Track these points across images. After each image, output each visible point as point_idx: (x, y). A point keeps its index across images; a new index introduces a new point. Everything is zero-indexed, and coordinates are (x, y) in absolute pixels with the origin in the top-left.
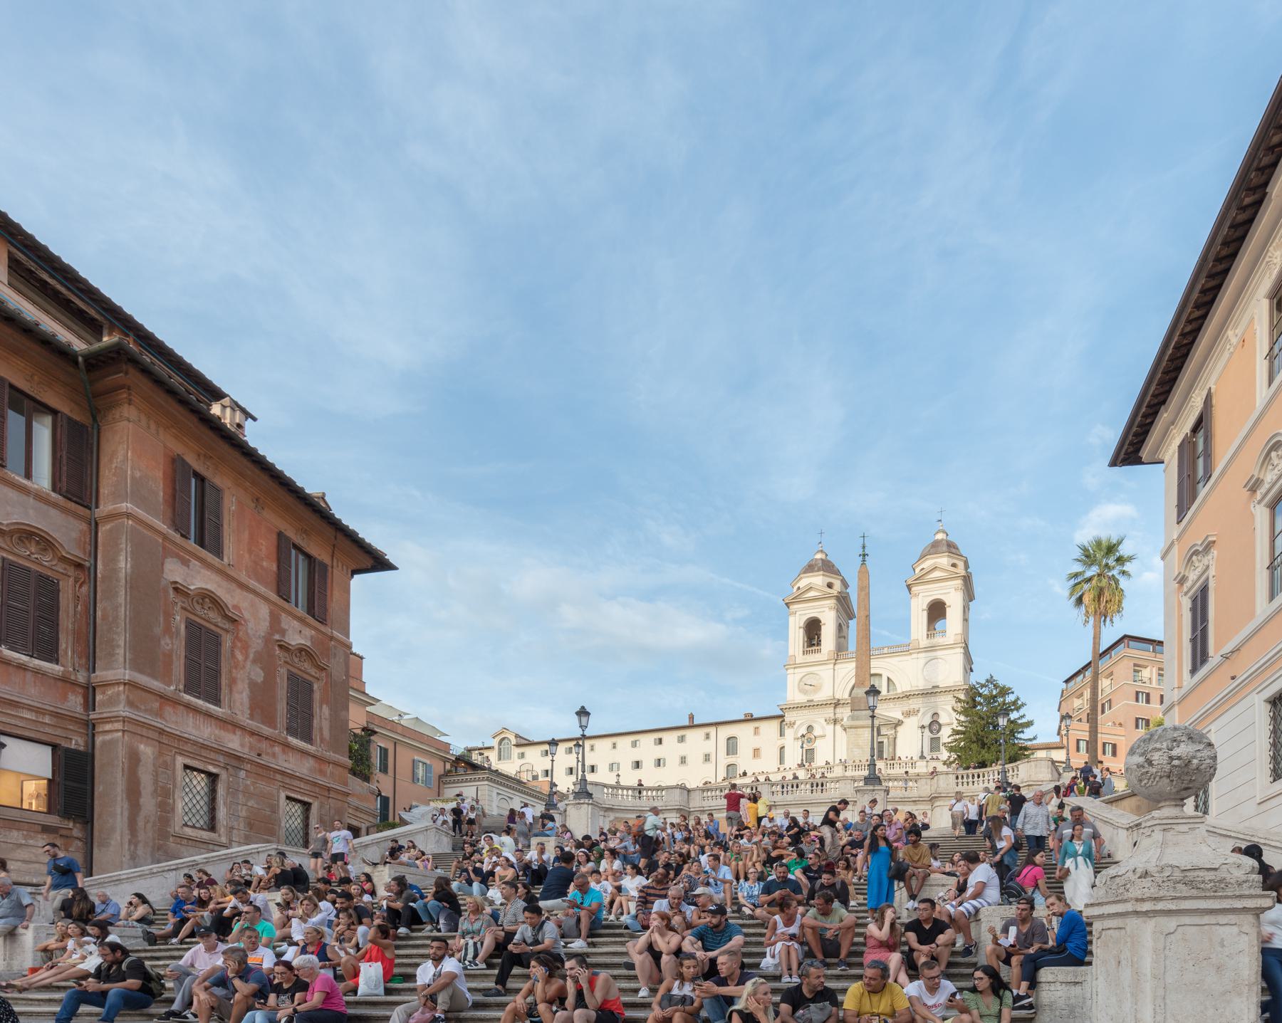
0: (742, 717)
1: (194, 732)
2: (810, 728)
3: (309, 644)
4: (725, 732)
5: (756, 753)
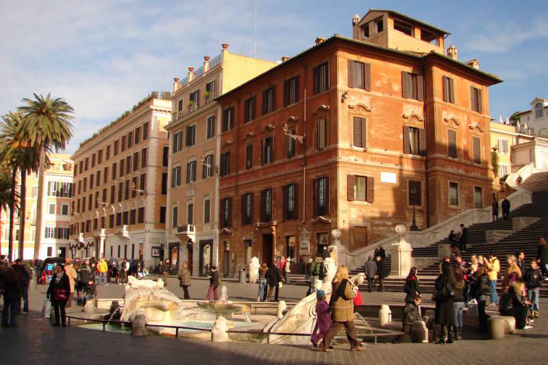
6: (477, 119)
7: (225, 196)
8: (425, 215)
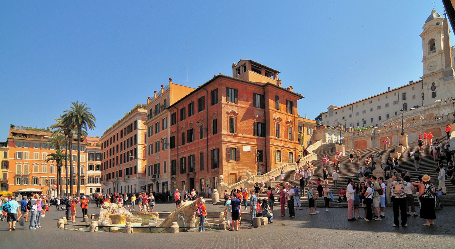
0: (408, 83)
1: (277, 144)
2: (433, 84)
3: (291, 120)
4: (401, 92)
5: (414, 97)
6: (291, 117)
7: (173, 159)
8: (265, 167)
